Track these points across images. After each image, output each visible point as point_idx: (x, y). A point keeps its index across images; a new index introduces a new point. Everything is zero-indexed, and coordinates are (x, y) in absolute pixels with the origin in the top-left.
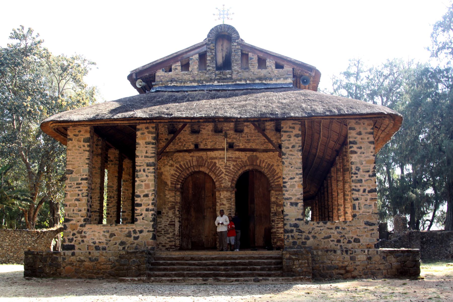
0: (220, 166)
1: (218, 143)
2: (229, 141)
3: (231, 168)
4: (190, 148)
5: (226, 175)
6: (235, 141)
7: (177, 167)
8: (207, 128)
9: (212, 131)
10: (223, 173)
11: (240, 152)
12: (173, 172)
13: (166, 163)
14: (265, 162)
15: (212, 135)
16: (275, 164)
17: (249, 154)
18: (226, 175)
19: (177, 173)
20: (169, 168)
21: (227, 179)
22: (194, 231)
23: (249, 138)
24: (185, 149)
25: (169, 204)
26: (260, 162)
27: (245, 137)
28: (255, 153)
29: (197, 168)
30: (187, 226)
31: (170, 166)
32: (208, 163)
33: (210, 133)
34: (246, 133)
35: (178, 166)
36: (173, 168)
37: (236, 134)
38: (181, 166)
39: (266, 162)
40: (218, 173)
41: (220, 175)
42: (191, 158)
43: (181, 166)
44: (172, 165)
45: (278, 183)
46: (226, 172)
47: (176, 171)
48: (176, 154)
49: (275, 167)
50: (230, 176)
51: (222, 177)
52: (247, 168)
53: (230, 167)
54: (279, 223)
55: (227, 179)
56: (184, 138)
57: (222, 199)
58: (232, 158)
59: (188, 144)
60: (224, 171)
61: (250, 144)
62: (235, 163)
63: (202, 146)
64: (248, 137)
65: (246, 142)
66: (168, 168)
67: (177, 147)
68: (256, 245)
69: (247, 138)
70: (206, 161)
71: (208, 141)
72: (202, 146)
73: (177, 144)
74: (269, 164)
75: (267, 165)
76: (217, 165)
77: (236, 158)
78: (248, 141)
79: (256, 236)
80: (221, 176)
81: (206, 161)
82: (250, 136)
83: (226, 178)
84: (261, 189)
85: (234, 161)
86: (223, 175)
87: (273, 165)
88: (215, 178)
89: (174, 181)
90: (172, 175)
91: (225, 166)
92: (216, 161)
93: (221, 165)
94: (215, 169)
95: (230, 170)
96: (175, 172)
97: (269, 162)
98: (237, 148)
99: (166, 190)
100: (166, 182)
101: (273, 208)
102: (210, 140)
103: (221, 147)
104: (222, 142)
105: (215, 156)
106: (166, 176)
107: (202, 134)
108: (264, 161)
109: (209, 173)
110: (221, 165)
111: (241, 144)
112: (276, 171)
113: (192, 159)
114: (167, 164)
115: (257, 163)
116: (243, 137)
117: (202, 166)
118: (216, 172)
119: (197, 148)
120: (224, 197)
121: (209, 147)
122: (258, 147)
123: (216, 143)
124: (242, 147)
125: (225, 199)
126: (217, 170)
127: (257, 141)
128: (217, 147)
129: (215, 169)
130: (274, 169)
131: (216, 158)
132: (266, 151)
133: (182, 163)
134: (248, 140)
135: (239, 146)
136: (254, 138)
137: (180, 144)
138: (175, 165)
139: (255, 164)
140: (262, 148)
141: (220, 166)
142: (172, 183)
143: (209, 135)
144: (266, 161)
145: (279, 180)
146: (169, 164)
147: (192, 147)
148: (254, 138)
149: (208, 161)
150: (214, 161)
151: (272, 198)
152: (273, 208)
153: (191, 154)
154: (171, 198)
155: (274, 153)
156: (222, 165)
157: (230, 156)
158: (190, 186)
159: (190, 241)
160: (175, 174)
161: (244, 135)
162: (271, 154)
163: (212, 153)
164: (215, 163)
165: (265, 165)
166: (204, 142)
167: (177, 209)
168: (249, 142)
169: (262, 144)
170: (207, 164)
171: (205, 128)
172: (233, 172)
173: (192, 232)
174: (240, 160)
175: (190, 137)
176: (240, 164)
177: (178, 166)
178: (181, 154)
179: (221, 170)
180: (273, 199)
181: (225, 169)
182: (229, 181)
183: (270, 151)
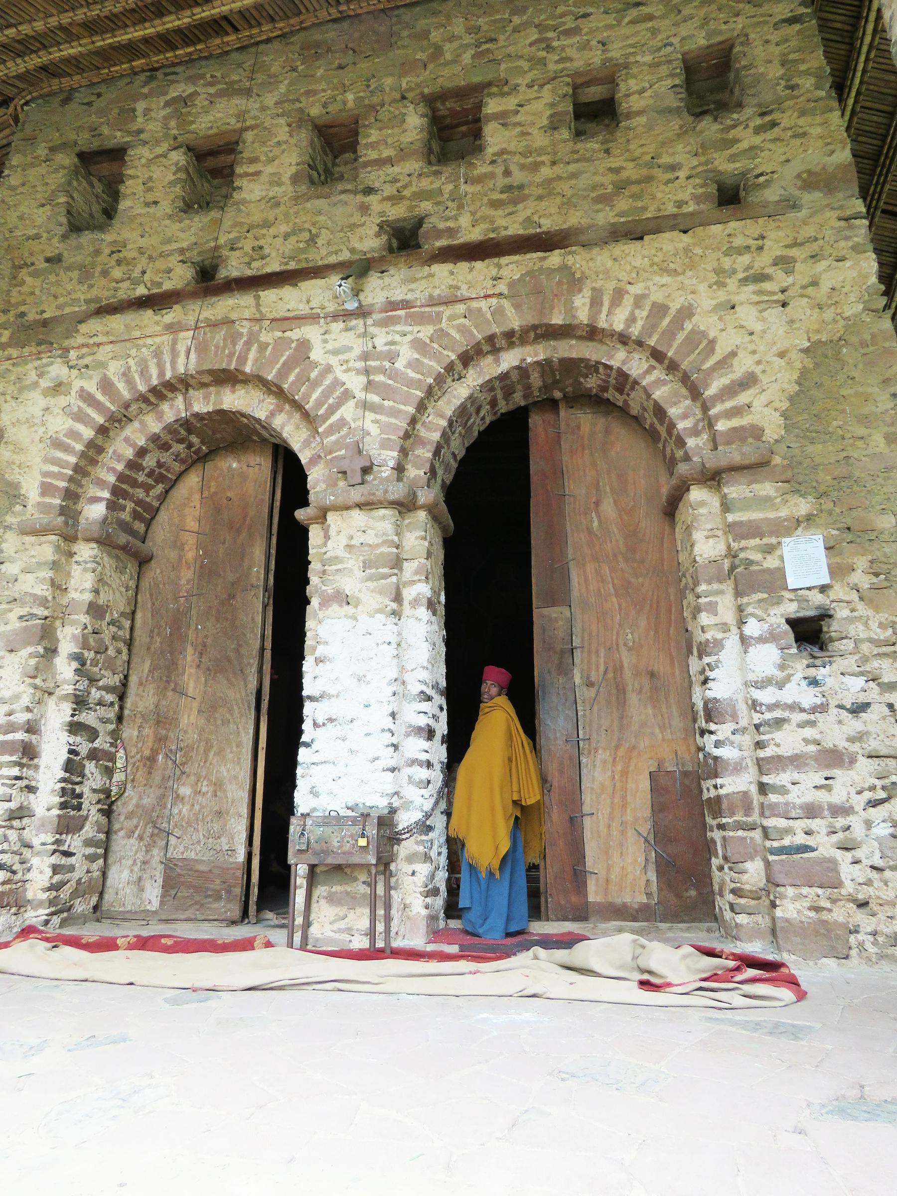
0: (334, 361)
1: (325, 236)
2: (397, 212)
3: (400, 364)
4: (167, 286)
5: (365, 406)
6: (426, 206)
7: (86, 397)
8: (270, 169)
9: (295, 179)
10: (347, 395)
11: (463, 266)
12: (59, 424)
13: (33, 376)
14: (628, 301)
15: (297, 199)
16: (705, 299)
17: (513, 267)
18: (365, 406)
19: (80, 427)
20: (42, 402)
21: (374, 430)
22: (185, 791)
23: (518, 177)
24: (141, 291)
25: (13, 616)
26: (596, 302)
27: (492, 175)
28: (555, 258)
29: (206, 398)
30: (152, 759)
31: (47, 393)
32: (263, 347)
33: (286, 190)
34: (503, 152)
35: (91, 386)
36: (62, 401)
37: (437, 173)
38: (106, 386)
39: (639, 301)
40: (319, 403)
41: (332, 410)
42: (167, 338)
43: (106, 386)
44: (58, 388)
45: (735, 422)
46: (370, 386)
47: (79, 417)
48: (94, 325)
49: (705, 321)
50: (394, 413)
51: (342, 423)
52: (509, 360)
53: (392, 357)
54: (779, 723)
55: (374, 430)
56: (143, 242)
57: (336, 560)
58: (406, 304)
59: (161, 264)
60: (355, 383)
61: (525, 211)
62: (426, 332)
63: (234, 267)
64: (507, 173)
65: (495, 204)
66: (35, 402)
67: (102, 291)
68: (594, 894)
69: (501, 181)
70: (248, 344)
71: (272, 231)
72: (234, 267)
73: (105, 273)
74: (660, 310)
75: (642, 314)
76: (316, 355)
77: (433, 302)
78: (515, 194)
79: (587, 822)
80: (334, 419)
81: (248, 344)
82: (523, 167)
83: (370, 424)
84: (608, 507)
85: (421, 319)
86: (347, 411)
87: (687, 312)
88: (306, 444)
89: (58, 476)
90: (57, 444)
91: (365, 356)
92: (312, 333)
93: (336, 352)
94: (303, 379)
95: (394, 375)
96: (70, 423)
97: (657, 296)
98: (439, 243)
99: (8, 528)
100: (17, 486)
101: (712, 609)
102: (284, 228)
103: (345, 256)
104: (353, 227)
105: (303, 309)
106: (18, 449)
107: (244, 202)
108: (619, 295)
109: (272, 414)
110: (336, 352)
111: (465, 221)
112: (712, 343)
113: (175, 342)
114: (36, 384)
115: (570, 309)
116: (479, 180)
117: (227, 378)
118: (307, 396)
119: (208, 280)
120: (349, 547)
121: (274, 266)
122: (574, 219)
123: (312, 240)
124: (471, 233)
125: (353, 563)
126: (316, 384)
127: (565, 187)
128: (321, 255)
129: (303, 379)
130: (696, 337)
131: (313, 318)
132: (634, 232)
133: (114, 370)
134: (509, 188)
135: (451, 232)
136: (546, 172)
137: (117, 273)
138: (77, 384)
139: (557, 319)
140: (606, 217)
141: (334, 361)
142: (46, 489)
143: (278, 204)
144: (636, 289)
145: (743, 398)
146: (45, 383)
147: (181, 276)
148: (546, 172)
149: (265, 337)
150: (295, 334)
151: (698, 536)
152: (712, 609)
153: (170, 316)
154: (30, 578)
155: (686, 239)
156: (349, 349)
157: (398, 295)
158: (192, 524)
159: (157, 854)
160: (74, 434)
161: (482, 168)
162: (669, 242)
163: (287, 292)
164: (304, 346)
165: (632, 319)
166: (247, 245)
167: (67, 645)
168: (515, 202)
169: (599, 200)
170: (252, 355)
171: (257, 173)
172: (411, 383)
173: (178, 798)
174: (461, 308)
175: (174, 228)
176: (461, 329)
177: (91, 386)
178: (116, 322)
179: (337, 383)
180: (707, 546)
181: (367, 372)
182: (385, 445)
183: (657, 231)
